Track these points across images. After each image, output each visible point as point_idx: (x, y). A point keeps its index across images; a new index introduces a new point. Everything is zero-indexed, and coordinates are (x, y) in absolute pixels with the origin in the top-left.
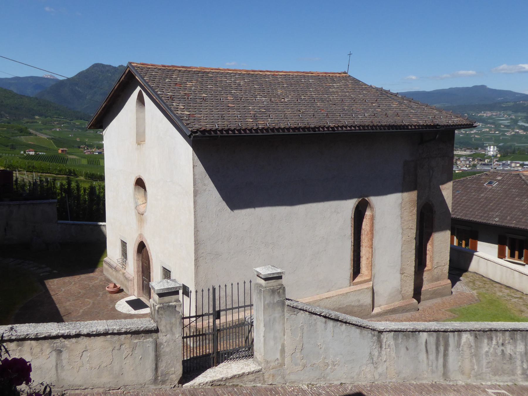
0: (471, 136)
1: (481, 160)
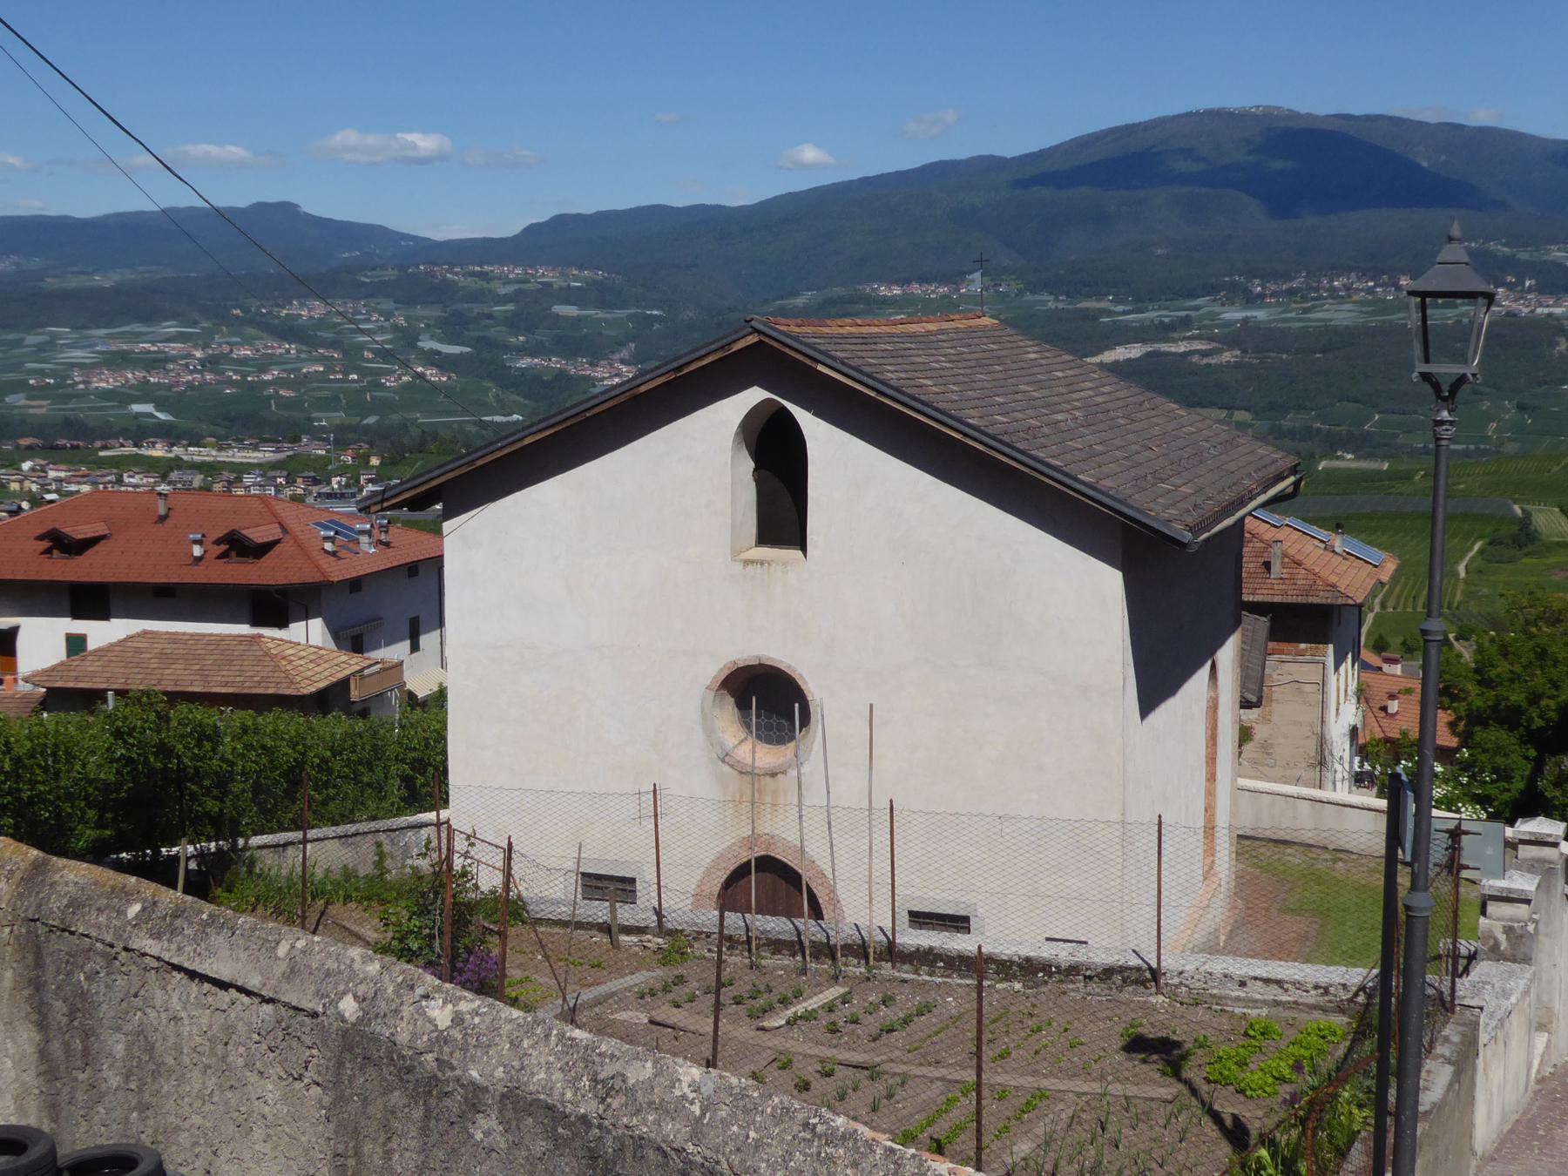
0: (265, 393)
1: (316, 482)
